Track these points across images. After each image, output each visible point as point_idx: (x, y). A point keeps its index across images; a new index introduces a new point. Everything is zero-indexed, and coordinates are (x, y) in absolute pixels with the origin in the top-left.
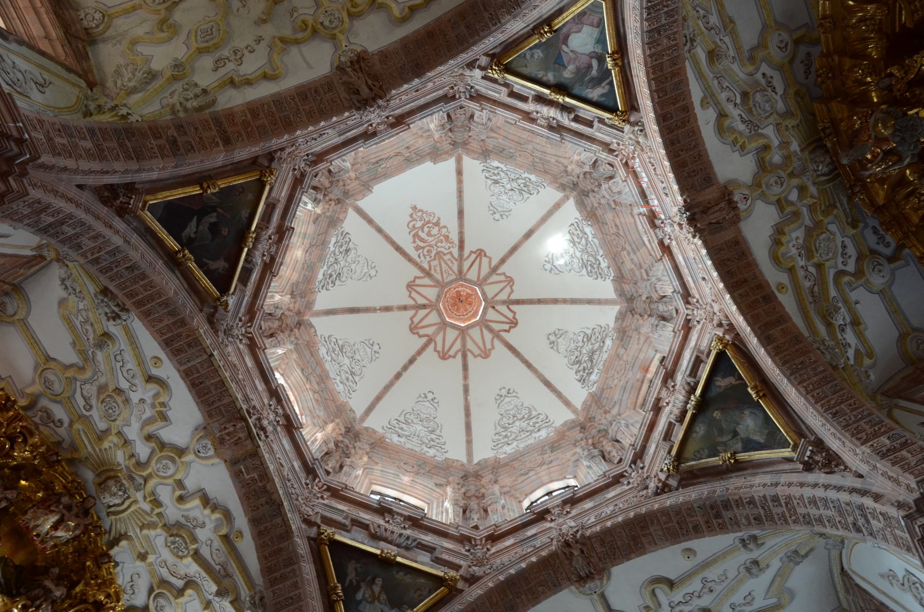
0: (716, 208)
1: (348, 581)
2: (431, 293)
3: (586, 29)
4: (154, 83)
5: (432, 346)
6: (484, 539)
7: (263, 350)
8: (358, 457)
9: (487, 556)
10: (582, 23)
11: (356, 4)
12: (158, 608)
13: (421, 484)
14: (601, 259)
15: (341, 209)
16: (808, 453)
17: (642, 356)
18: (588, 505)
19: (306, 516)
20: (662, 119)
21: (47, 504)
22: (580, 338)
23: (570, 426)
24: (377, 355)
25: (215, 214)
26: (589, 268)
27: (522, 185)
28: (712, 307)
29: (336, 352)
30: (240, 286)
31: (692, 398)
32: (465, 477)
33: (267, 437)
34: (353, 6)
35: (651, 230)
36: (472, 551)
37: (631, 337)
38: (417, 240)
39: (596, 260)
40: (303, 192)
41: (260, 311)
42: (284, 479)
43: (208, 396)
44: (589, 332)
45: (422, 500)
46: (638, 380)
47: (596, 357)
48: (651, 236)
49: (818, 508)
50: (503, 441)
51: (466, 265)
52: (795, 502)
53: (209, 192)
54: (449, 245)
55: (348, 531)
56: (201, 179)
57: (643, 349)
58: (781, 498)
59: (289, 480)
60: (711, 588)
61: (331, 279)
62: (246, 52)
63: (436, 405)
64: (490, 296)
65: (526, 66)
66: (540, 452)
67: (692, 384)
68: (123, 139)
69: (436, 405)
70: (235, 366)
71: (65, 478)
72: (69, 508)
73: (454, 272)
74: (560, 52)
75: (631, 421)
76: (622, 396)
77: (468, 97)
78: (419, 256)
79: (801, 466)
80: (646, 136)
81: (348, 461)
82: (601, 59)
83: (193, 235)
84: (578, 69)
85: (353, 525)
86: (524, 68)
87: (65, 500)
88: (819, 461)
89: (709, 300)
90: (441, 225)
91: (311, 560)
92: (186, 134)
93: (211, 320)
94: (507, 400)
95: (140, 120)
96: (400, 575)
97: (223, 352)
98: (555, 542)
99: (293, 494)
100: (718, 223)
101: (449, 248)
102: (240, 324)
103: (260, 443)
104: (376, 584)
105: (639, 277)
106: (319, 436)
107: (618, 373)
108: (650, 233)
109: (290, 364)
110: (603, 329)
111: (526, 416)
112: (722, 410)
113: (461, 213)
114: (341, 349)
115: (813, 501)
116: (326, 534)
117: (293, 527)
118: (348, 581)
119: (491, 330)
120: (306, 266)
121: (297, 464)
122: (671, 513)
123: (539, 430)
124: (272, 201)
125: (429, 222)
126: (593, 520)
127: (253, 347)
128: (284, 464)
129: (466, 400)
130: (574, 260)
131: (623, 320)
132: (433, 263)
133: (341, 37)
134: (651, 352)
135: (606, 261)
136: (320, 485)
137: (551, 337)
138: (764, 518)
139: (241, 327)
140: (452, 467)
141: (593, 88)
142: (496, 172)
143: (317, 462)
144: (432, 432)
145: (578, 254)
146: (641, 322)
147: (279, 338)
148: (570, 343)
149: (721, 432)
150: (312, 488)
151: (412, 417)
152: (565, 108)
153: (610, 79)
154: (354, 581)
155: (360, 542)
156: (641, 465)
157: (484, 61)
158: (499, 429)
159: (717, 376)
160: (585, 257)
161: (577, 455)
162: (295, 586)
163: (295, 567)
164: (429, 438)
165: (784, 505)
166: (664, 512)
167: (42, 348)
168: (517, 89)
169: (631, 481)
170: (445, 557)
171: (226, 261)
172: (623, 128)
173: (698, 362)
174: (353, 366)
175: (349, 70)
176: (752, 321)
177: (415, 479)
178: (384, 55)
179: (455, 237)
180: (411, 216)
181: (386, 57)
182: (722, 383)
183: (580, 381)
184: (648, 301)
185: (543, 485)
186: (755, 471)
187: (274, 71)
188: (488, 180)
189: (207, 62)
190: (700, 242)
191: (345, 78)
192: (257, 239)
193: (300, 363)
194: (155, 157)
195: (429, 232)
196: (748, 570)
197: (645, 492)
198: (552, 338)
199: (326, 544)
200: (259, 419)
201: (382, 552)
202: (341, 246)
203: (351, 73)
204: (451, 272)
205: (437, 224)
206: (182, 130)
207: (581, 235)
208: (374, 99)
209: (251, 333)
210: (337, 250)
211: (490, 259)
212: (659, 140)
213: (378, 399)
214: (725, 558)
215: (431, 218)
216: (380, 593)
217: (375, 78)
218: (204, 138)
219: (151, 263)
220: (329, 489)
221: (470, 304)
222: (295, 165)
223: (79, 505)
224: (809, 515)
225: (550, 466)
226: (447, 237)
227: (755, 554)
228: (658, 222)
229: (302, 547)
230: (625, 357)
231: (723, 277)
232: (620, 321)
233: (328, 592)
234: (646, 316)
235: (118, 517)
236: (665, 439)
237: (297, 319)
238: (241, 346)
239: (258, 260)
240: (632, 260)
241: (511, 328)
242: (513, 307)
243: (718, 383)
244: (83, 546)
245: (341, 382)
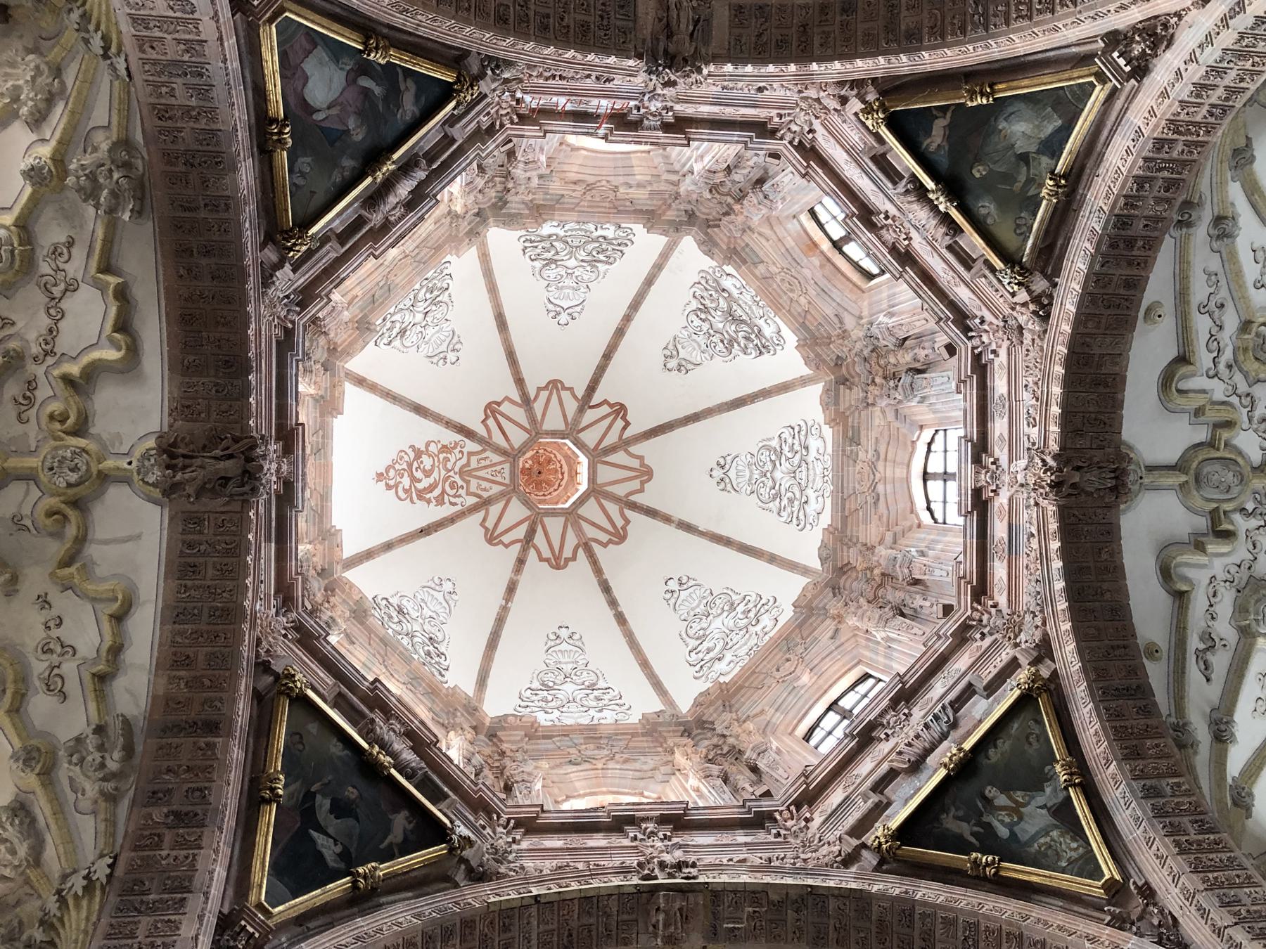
0: (674, 13)
1: (973, 840)
2: (516, 511)
3: (309, 66)
4: (37, 811)
5: (597, 548)
6: (975, 605)
7: (543, 811)
8: (743, 737)
9: (1006, 611)
10: (298, 66)
11: (61, 414)
13: (823, 659)
14: (600, 232)
15: (343, 591)
16: (1122, 62)
17: (790, 243)
18: (999, 427)
19: (839, 859)
20: (502, 23)
22: (697, 322)
23: (831, 400)
24: (576, 637)
25: (319, 797)
26: (601, 257)
27: (428, 296)
28: (806, 98)
29: (550, 698)
30: (443, 805)
31: (931, 196)
32: (836, 590)
33: (694, 865)
34: (63, 422)
35: (641, 133)
36: (986, 631)
37: (747, 245)
38: (428, 496)
39: (596, 240)
40: (325, 639)
41: (480, 790)
42: (767, 867)
43: (594, 933)
44: (695, 304)
45: (849, 670)
46: (822, 266)
47: (740, 312)
48: (649, 137)
50: (795, 509)
51: (498, 439)
52: (1182, 117)
53: (281, 792)
54: (457, 451)
55: (889, 804)
56: (253, 801)
57: (780, 236)
58: (1164, 136)
59: (770, 860)
60: (1218, 305)
61: (433, 655)
62: (55, 633)
63: (691, 583)
64: (561, 427)
65: (313, 193)
66: (851, 462)
67: (910, 186)
68: (142, 902)
69: (691, 583)
70: (560, 867)
73: (500, 463)
74: (321, 128)
75: (884, 306)
76: (834, 300)
77: (298, 309)
78: (454, 504)
79: (1133, 81)
80: (509, 64)
81: (749, 754)
82: (365, 68)
83: (338, 849)
84: (360, 113)
85: (882, 793)
86: (316, 196)
88: (1144, 51)
89: (796, 97)
90: (423, 449)
91: (915, 881)
92: (169, 791)
93: (478, 876)
94: (732, 474)
95: (111, 861)
96: (994, 755)
97: (535, 877)
98: (1044, 503)
99: (794, 864)
100: (696, 23)
101: (461, 452)
102: (488, 830)
103: (701, 879)
104: (995, 797)
105: (671, 187)
106: (693, 781)
107: (792, 291)
108: (644, 137)
109: (555, 779)
110: (703, 282)
111: (773, 458)
112: (977, 160)
113: (419, 410)
114: (549, 689)
115: (1201, 88)
116: (883, 840)
117: (853, 886)
118: (973, 840)
119: (613, 449)
120: (409, 686)
121: (741, 837)
122: (1088, 311)
123: (807, 448)
124: (332, 696)
125: (410, 465)
126: (1034, 433)
127: (530, 826)
128: (742, 857)
129: (702, 534)
130: (576, 274)
131: (716, 244)
132: (473, 489)
133: (110, 463)
134: (793, 226)
135: (608, 226)
136: (786, 814)
137: (669, 366)
138: (1174, 176)
139: (495, 833)
140: (811, 601)
141: (399, 106)
142: (388, 325)
143: (748, 804)
144: (732, 607)
145: (572, 263)
146: (740, 219)
147: (519, 779)
148: (694, 340)
149: (1009, 178)
150: (786, 829)
151: (696, 626)
152: (406, 168)
153: (400, 71)
154: (976, 829)
155: (915, 793)
156: (977, 321)
157: (271, 255)
158: (774, 506)
159: (922, 143)
160: (582, 255)
161: (887, 410)
162: (950, 923)
163: (919, 910)
164: (741, 616)
165: (1175, 136)
166: (1081, 320)
168: (338, 226)
169: (994, 347)
170: (990, 671)
171: (397, 812)
172: (481, 93)
173: (882, 161)
174: (581, 681)
175: (179, 476)
176: (873, 50)
177: (811, 666)
178: (182, 408)
179: (450, 437)
180: (389, 487)
181: (188, 407)
182: (936, 140)
183: (761, 353)
184: (714, 191)
185: (907, 480)
187: (116, 599)
188: (392, 345)
189: (40, 705)
190: (712, 68)
191: (190, 489)
192: (384, 746)
193: (558, 761)
194: (194, 859)
195: (424, 471)
197: (1028, 337)
198: (673, 364)
199: (899, 847)
200: (662, 865)
201: (945, 766)
202: (391, 617)
203: (186, 476)
204: (498, 468)
205: (419, 454)
206: (161, 795)
207: (547, 244)
208: (249, 460)
209: (509, 820)
210: (394, 626)
211: (507, 398)
212: (529, 46)
213: (645, 665)
214: (1188, 263)
215: (406, 458)
216: (1010, 798)
217: (214, 439)
218: (190, 764)
219: (358, 939)
220: (798, 804)
221: (549, 461)
222: (281, 634)
224: (1213, 106)
225: (882, 456)
226: (445, 449)
227: (1207, 215)
228: (634, 115)
229: (890, 885)
230: (773, 269)
231: (781, 60)
232: (716, 251)
233: (977, 877)
234: (737, 207)
236: (968, 268)
237: (482, 737)
238: (525, 845)
239: (409, 756)
240: (639, 185)
241: (624, 418)
242: (596, 399)
243: (933, 148)
245: (601, 711)
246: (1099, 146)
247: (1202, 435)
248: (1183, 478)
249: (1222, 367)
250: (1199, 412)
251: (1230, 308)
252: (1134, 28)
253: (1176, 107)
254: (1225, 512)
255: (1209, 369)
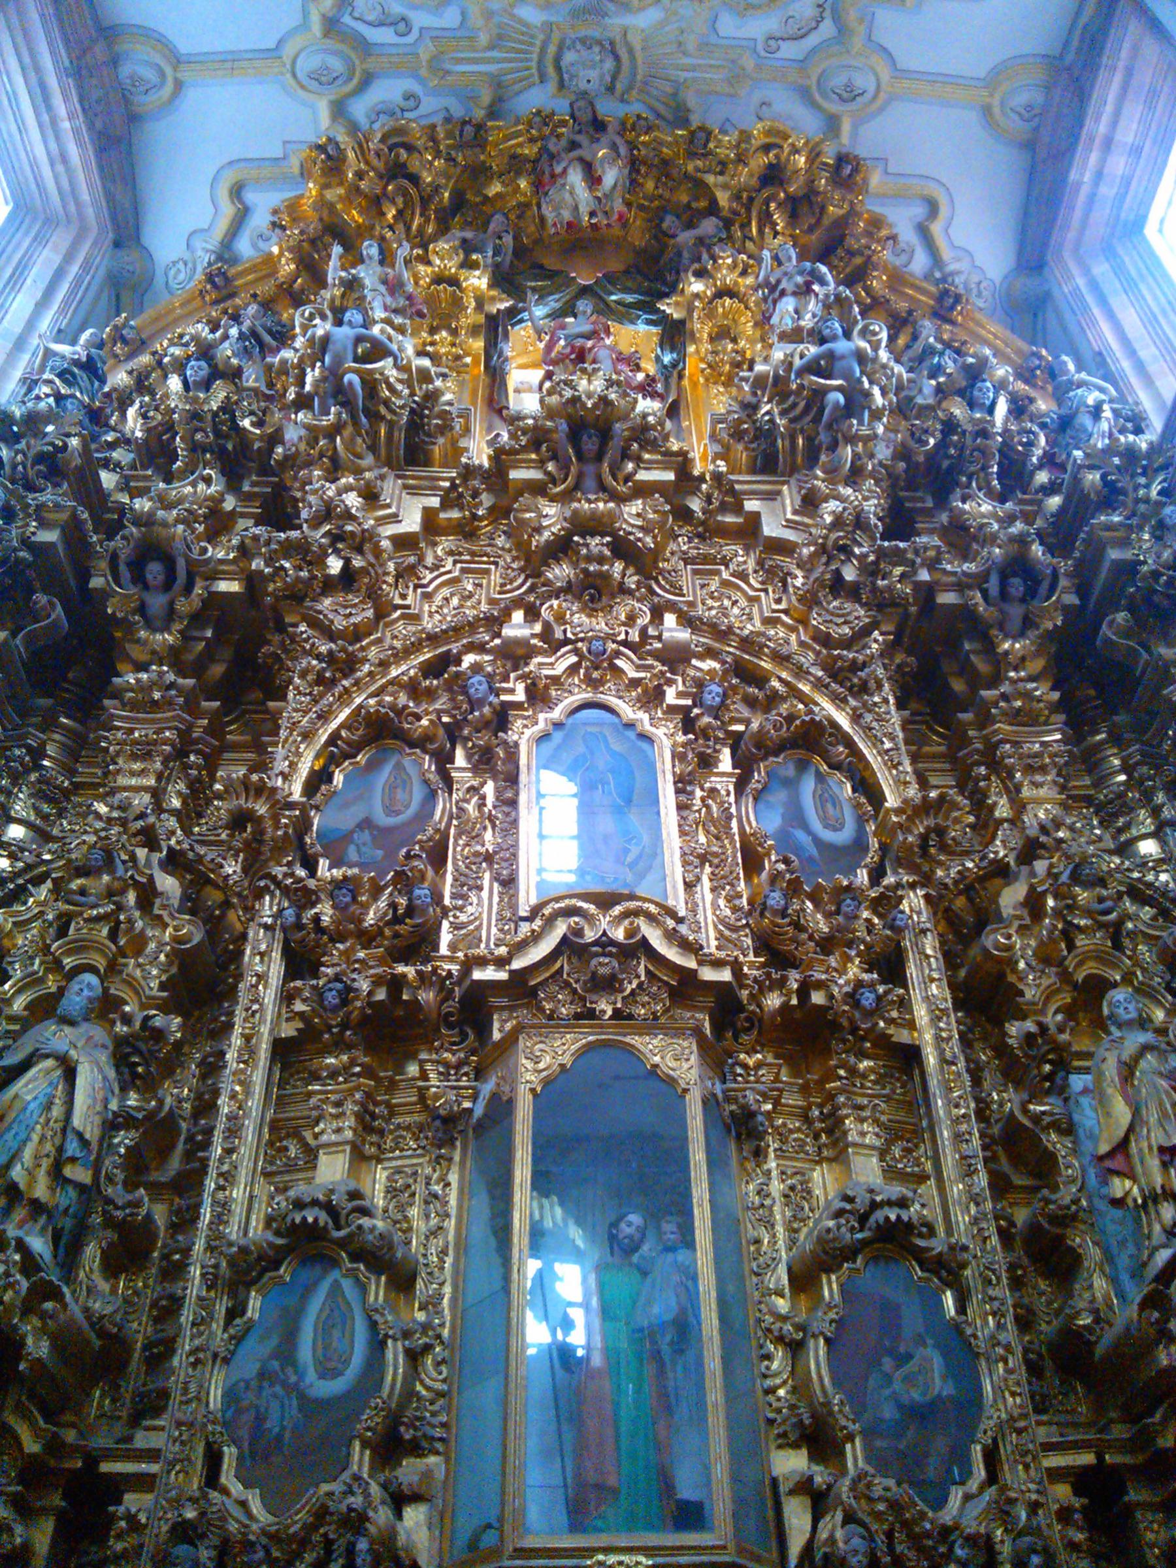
12: (845, 95)
21: (547, 175)
71: (519, 134)
72: (574, 145)
87: (553, 146)
167: (250, 56)
223: (577, 128)
235: (638, 85)
244: (656, 161)
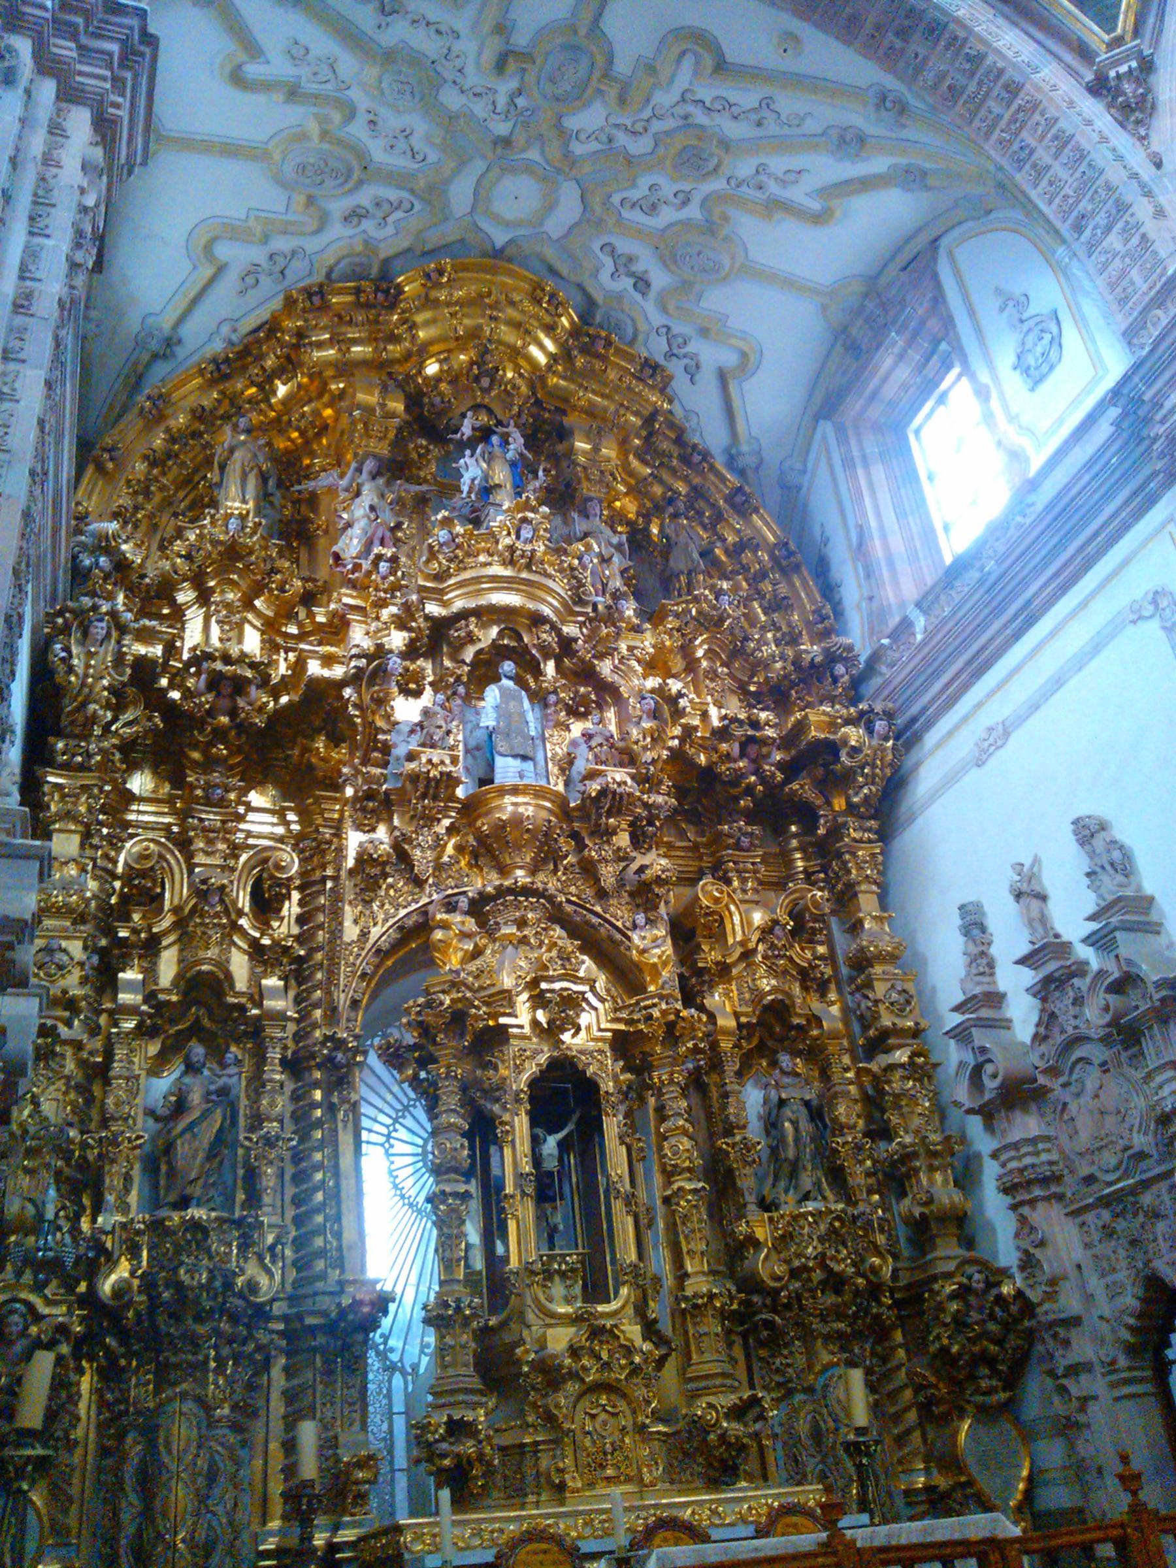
16: (1123, 69)
49: (1056, 156)
52: (1037, 117)
58: (1022, 95)
88: (1124, 94)
115: (1063, 141)
138: (965, 96)
165: (1014, 107)
186: (1015, 18)
196: (843, 142)
224: (1031, 152)
246: (1023, 23)
247: (622, 67)
248: (582, 31)
249: (689, 108)
250: (651, 70)
251: (753, 133)
252: (1149, 90)
253: (1052, 112)
254: (524, 70)
255: (662, 107)
